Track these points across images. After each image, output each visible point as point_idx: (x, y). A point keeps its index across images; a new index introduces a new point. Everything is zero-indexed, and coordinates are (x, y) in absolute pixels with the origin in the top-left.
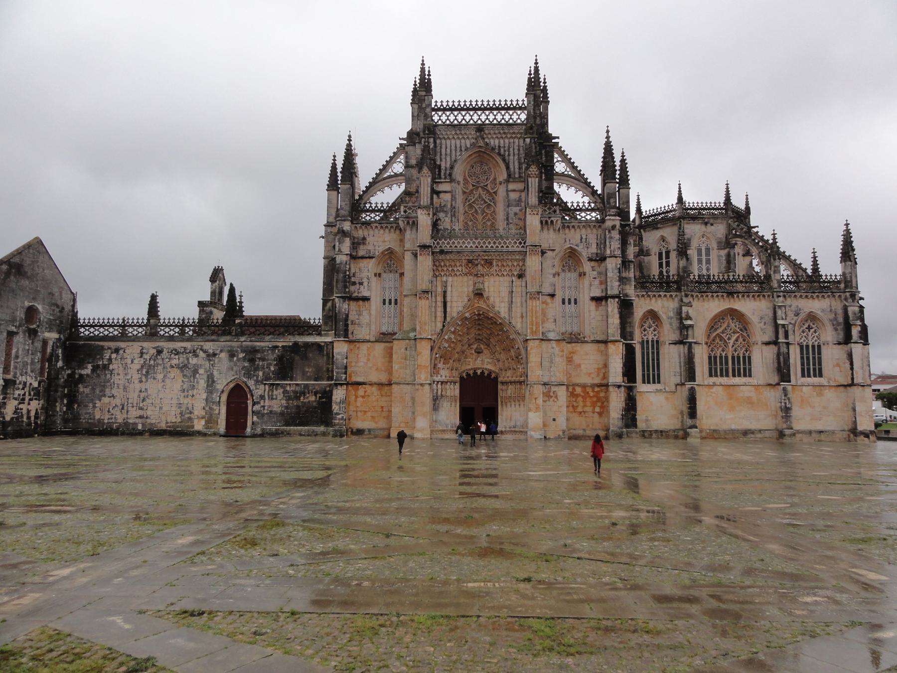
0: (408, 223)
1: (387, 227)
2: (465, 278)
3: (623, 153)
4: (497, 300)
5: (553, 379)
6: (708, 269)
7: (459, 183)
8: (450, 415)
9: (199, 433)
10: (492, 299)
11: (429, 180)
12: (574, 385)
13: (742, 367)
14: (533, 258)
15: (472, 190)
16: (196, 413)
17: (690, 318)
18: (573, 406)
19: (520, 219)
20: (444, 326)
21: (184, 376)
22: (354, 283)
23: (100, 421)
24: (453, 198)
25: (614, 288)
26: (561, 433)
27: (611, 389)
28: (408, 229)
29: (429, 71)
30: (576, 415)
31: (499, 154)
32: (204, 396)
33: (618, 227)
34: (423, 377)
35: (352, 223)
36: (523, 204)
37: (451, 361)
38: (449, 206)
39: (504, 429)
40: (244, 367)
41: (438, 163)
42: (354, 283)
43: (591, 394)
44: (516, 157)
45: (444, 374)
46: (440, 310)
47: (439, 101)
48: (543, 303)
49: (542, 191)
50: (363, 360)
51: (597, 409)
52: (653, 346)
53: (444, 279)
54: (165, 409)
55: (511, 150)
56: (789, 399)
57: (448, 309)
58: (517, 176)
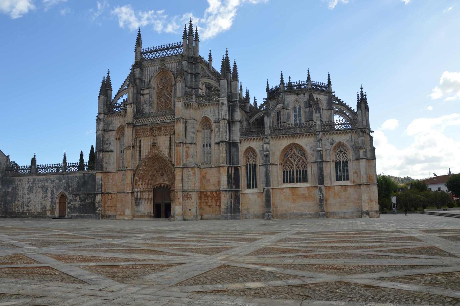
2: (150, 138)
4: (164, 148)
5: (189, 188)
6: (300, 120)
9: (48, 216)
13: (302, 176)
14: (179, 124)
16: (47, 208)
17: (268, 150)
18: (206, 202)
21: (43, 191)
22: (107, 144)
23: (14, 212)
27: (221, 192)
30: (207, 207)
32: (50, 200)
34: (128, 189)
35: (105, 114)
37: (147, 180)
40: (65, 186)
43: (215, 195)
45: (142, 187)
46: (138, 154)
48: (187, 148)
50: (111, 181)
51: (218, 204)
54: (36, 206)
56: (322, 194)
57: (142, 154)
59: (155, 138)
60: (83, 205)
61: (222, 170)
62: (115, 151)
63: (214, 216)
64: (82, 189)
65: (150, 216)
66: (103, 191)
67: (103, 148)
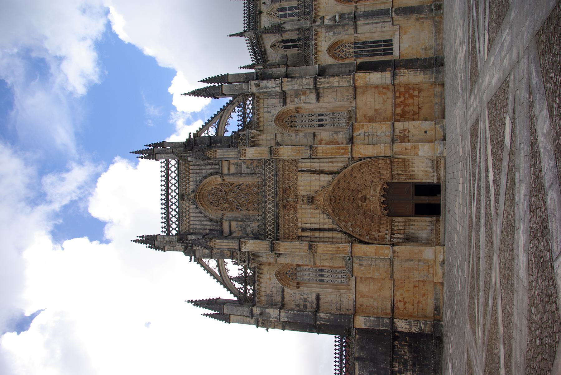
0: (253, 259)
1: (258, 277)
2: (300, 211)
3: (201, 81)
4: (318, 183)
5: (388, 134)
7: (223, 215)
8: (422, 226)
10: (317, 188)
11: (218, 241)
12: (395, 114)
14: (281, 152)
15: (229, 204)
17: (334, 17)
18: (413, 115)
19: (252, 164)
20: (341, 231)
22: (305, 306)
24: (235, 219)
25: (308, 82)
26: (438, 126)
28: (258, 259)
29: (140, 237)
31: (200, 181)
33: (256, 82)
34: (386, 252)
35: (254, 306)
36: (240, 161)
38: (241, 223)
39: (435, 177)
41: (208, 231)
42: (305, 306)
44: (204, 168)
46: (326, 234)
47: (161, 229)
49: (229, 145)
50: (371, 302)
51: (416, 93)
52: (359, 48)
53: (300, 230)
55: (198, 171)
57: (326, 227)
58: (217, 167)
59: (300, 200)
60: (414, 364)
61: (359, 82)
62: (318, 290)
63: (437, 100)
64: (383, 366)
65: (438, 221)
66: (389, 317)
67: (311, 312)
